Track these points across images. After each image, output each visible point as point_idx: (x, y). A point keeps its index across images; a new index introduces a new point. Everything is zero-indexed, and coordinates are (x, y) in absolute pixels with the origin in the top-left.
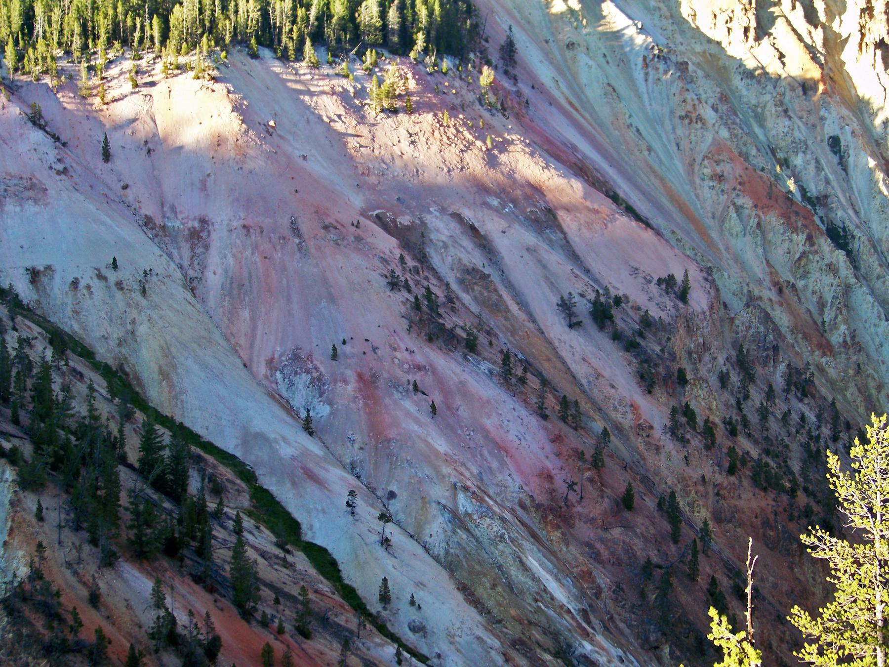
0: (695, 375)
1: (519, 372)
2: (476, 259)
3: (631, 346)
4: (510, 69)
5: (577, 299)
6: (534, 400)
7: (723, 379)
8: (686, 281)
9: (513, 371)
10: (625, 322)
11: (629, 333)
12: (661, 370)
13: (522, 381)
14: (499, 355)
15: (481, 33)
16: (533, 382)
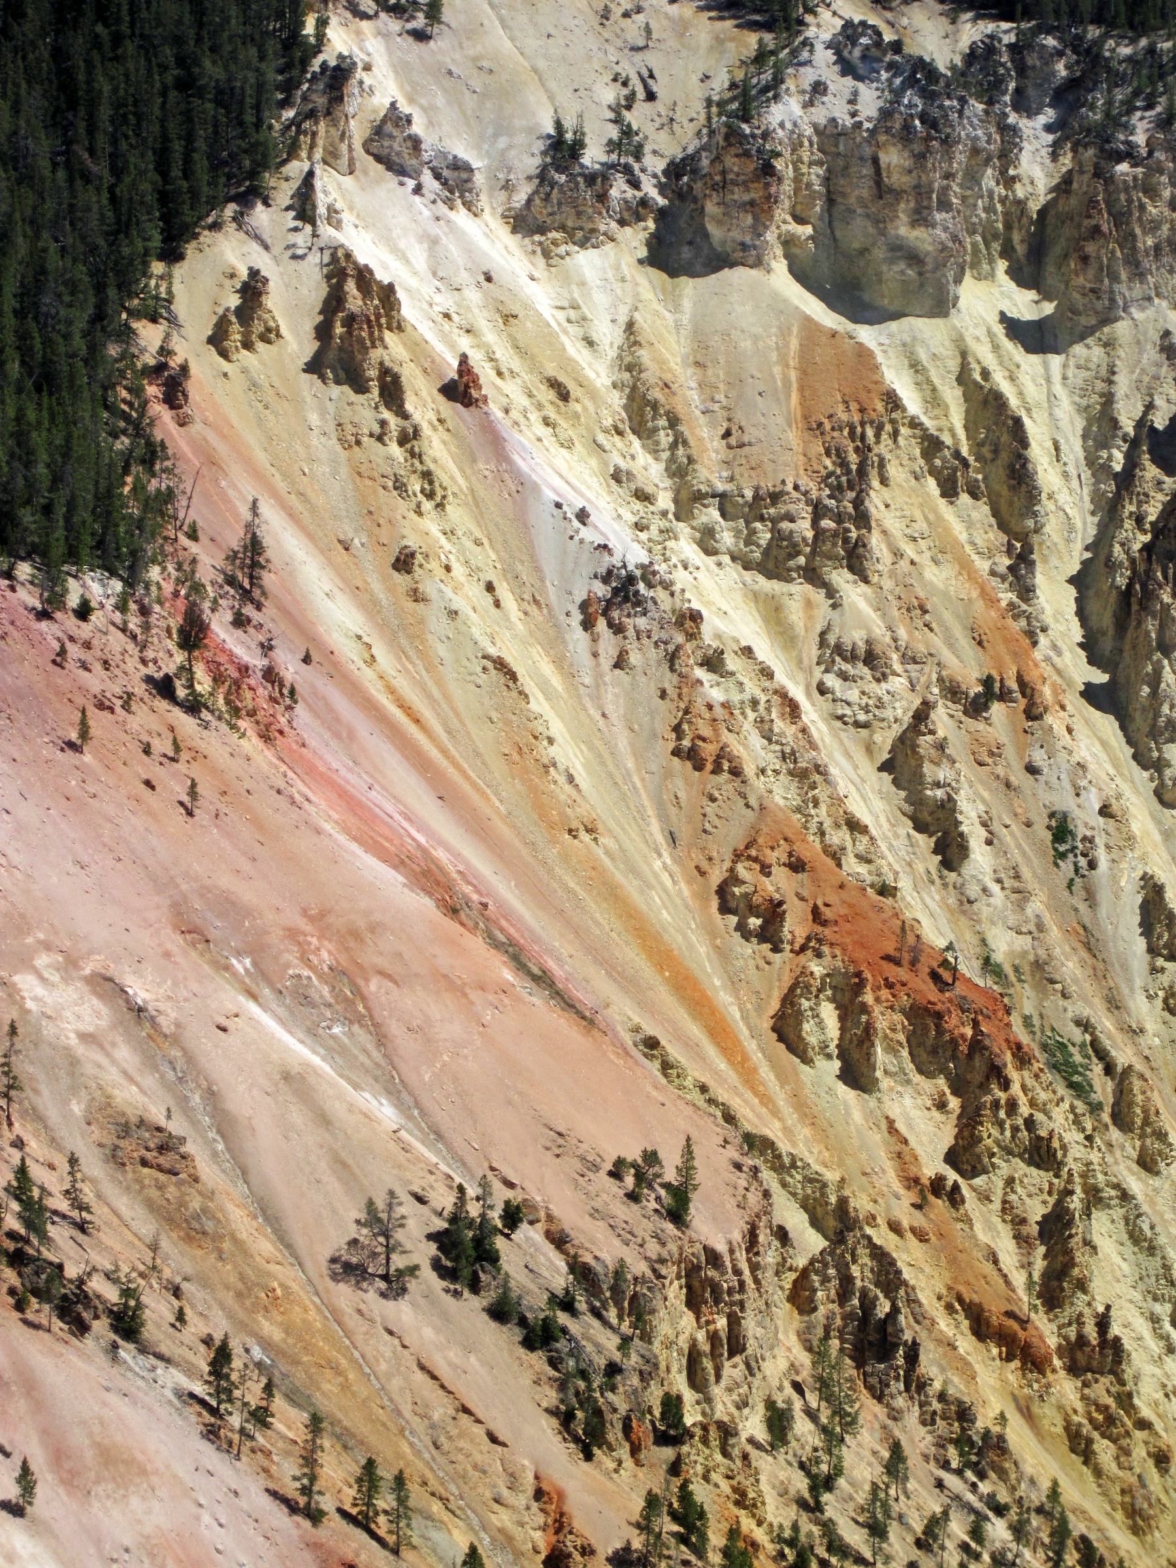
0: (704, 1414)
1: (253, 1393)
2: (145, 1098)
3: (540, 1336)
4: (249, 610)
5: (408, 1207)
6: (288, 1472)
7: (778, 1422)
8: (687, 1169)
9: (237, 1393)
10: (530, 1265)
11: (535, 1304)
12: (619, 1401)
13: (261, 1416)
14: (202, 1348)
15: (181, 515)
16: (289, 1421)
